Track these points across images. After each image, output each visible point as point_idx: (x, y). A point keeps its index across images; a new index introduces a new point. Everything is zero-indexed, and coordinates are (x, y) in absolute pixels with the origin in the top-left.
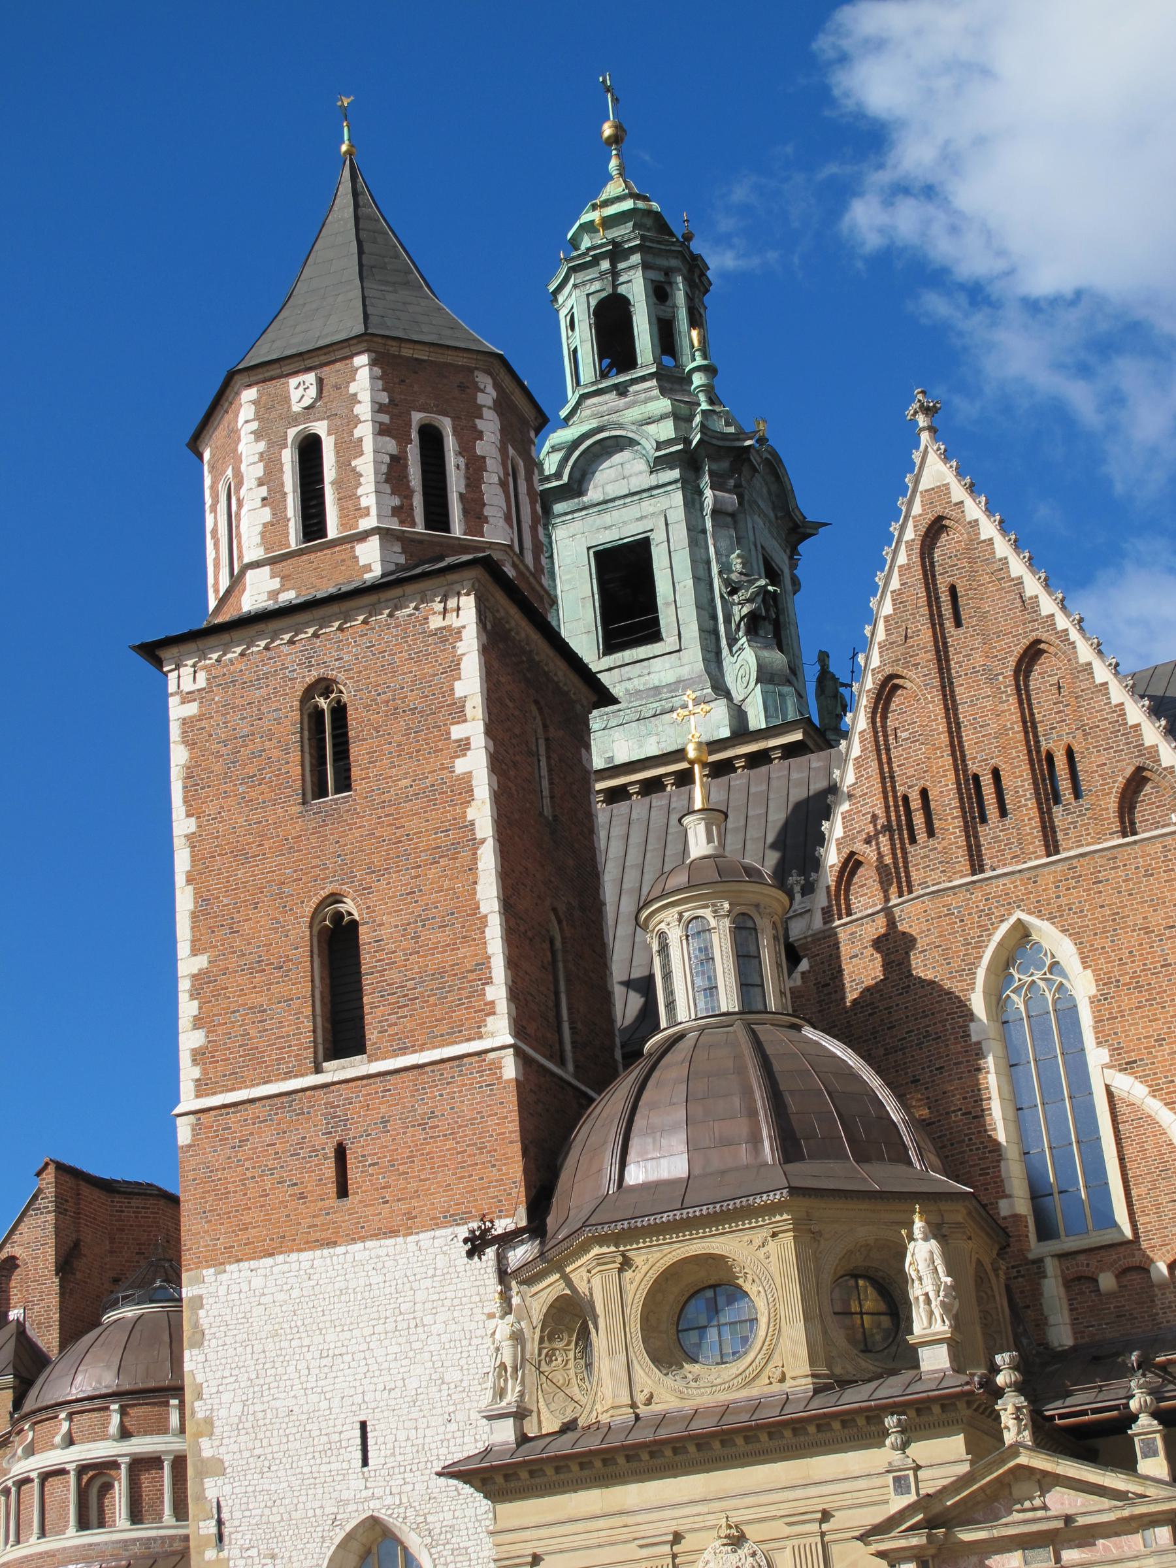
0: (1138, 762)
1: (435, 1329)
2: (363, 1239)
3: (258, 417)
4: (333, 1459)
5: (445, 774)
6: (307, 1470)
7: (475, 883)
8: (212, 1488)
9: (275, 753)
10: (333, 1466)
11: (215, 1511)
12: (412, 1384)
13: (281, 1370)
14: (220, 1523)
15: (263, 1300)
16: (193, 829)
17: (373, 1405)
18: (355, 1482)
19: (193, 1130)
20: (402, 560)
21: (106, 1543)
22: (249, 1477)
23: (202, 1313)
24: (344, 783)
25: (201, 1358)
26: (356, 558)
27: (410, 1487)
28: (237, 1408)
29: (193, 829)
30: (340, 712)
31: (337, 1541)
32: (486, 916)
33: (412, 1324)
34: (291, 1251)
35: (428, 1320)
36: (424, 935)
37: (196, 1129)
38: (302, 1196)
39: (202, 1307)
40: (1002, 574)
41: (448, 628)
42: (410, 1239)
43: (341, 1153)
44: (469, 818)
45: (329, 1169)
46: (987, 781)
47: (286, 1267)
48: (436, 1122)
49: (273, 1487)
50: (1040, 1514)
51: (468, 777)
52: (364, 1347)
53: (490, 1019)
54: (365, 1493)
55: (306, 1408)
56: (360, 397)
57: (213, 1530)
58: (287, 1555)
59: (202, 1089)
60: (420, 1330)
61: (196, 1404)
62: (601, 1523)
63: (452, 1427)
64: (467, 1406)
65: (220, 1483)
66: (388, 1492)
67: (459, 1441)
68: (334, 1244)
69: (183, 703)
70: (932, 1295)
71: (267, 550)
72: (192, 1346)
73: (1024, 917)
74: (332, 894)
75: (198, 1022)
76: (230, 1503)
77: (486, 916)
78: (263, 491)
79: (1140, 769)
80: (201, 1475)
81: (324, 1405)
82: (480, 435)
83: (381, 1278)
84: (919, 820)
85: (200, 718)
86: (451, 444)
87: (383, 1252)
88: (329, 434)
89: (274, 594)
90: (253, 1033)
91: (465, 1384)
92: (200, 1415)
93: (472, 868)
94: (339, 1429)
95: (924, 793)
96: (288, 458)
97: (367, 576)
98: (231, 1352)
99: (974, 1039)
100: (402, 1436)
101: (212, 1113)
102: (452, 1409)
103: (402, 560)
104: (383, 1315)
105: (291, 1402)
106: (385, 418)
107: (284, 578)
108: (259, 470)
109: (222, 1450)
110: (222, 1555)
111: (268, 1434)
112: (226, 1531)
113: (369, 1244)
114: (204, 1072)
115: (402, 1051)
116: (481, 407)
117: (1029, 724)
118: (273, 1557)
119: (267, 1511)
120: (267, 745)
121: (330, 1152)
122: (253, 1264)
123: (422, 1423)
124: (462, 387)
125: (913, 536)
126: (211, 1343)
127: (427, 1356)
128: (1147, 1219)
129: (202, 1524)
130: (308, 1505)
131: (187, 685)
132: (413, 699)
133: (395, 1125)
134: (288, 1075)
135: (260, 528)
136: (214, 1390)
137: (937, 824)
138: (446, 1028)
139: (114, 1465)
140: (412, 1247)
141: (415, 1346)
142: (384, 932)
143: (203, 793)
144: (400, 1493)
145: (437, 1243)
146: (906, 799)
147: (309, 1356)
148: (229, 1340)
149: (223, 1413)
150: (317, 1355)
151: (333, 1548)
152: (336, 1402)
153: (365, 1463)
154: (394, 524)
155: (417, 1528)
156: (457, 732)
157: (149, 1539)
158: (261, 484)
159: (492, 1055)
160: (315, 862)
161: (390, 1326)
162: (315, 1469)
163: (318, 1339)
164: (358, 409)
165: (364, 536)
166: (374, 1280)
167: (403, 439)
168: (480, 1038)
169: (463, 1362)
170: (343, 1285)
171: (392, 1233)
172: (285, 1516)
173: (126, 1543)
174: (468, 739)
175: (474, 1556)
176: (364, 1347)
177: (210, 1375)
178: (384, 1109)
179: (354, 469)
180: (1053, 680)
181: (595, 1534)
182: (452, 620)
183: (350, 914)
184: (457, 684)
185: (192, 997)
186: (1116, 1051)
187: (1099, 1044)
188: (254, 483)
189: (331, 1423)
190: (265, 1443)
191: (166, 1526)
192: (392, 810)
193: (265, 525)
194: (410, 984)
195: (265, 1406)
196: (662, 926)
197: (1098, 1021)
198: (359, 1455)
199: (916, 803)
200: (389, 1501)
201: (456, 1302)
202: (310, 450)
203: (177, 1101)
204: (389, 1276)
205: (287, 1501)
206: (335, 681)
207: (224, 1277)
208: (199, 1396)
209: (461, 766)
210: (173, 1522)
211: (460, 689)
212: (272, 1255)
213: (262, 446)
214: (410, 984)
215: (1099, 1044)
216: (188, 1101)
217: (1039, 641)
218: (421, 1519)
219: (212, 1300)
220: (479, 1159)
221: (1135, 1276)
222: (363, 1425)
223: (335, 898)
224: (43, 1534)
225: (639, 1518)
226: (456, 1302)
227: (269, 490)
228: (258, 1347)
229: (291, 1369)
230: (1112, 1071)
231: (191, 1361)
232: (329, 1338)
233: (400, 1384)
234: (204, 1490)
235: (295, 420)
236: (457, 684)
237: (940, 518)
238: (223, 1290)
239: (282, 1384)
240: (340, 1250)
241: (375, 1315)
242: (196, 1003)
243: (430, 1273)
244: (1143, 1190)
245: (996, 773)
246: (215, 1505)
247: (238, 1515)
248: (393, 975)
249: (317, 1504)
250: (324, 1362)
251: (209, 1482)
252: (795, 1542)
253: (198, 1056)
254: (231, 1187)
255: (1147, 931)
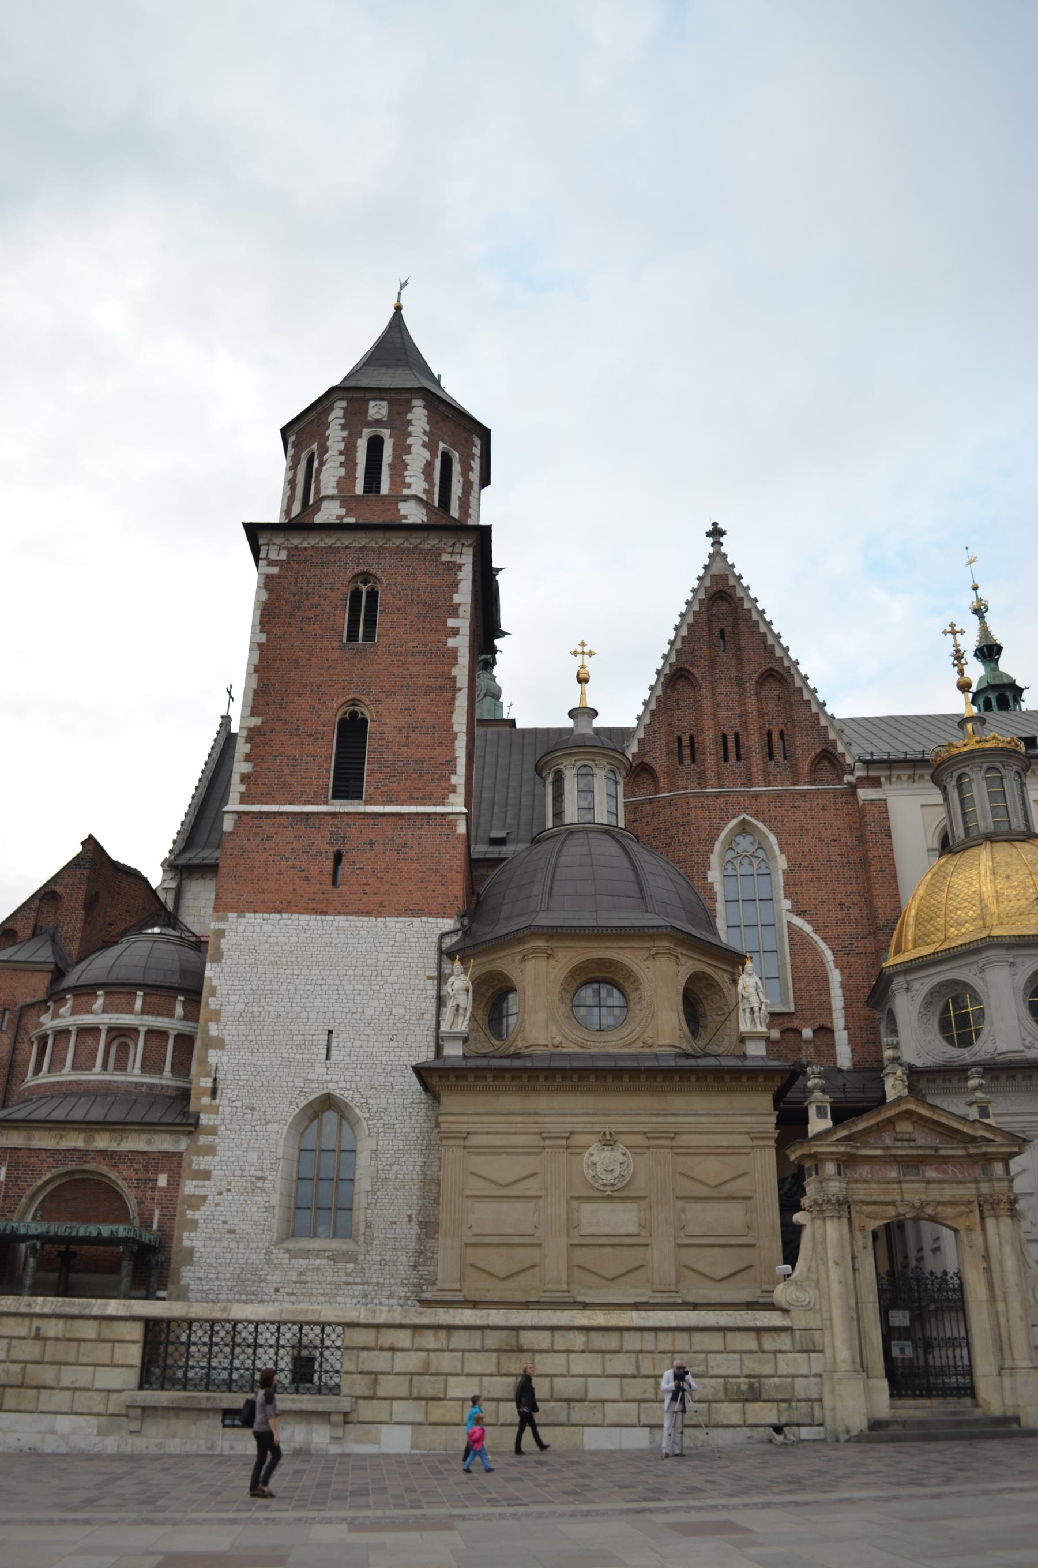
0: (824, 746)
1: (390, 979)
2: (346, 914)
3: (345, 417)
4: (306, 1051)
5: (440, 645)
6: (285, 1055)
7: (452, 712)
8: (213, 1057)
9: (328, 609)
10: (305, 1056)
11: (213, 1072)
12: (370, 1012)
13: (276, 987)
14: (215, 1080)
15: (270, 940)
16: (264, 640)
17: (338, 1021)
18: (320, 1069)
19: (235, 823)
20: (425, 519)
21: (122, 1082)
22: (242, 1053)
23: (223, 941)
24: (370, 636)
25: (218, 970)
26: (398, 510)
27: (358, 1078)
28: (240, 1007)
29: (264, 640)
30: (373, 595)
31: (301, 1106)
32: (456, 734)
33: (374, 973)
34: (294, 912)
35: (386, 972)
36: (413, 736)
37: (237, 824)
38: (307, 879)
39: (224, 937)
40: (754, 629)
41: (454, 562)
42: (379, 919)
43: (338, 858)
44: (453, 673)
45: (328, 865)
46: (731, 738)
47: (289, 922)
48: (407, 850)
49: (259, 1063)
50: (912, 1144)
51: (455, 651)
52: (338, 982)
53: (451, 796)
54: (326, 1078)
55: (290, 1015)
56: (413, 422)
57: (210, 1085)
58: (263, 1109)
59: (244, 799)
60: (379, 978)
61: (210, 999)
62: (519, 1119)
63: (394, 1044)
64: (406, 1032)
65: (220, 1054)
66: (342, 1078)
67: (398, 1054)
68: (326, 913)
69: (268, 565)
70: (756, 1009)
71: (339, 491)
72: (212, 961)
73: (748, 818)
74: (354, 699)
75: (248, 758)
76: (226, 1068)
77: (456, 734)
78: (342, 458)
79: (824, 750)
80: (206, 1047)
81: (304, 1015)
82: (472, 469)
83: (356, 941)
84: (686, 752)
85: (279, 576)
86: (456, 468)
87: (359, 924)
88: (391, 437)
89: (339, 517)
90: (287, 772)
91: (407, 1018)
92: (212, 1007)
93: (451, 703)
94: (312, 1032)
95: (692, 738)
96: (362, 445)
97: (404, 521)
98: (241, 969)
99: (710, 880)
100: (358, 1043)
101: (250, 816)
102: (395, 1032)
103: (425, 519)
104: (354, 964)
105: (280, 1010)
106: (427, 439)
107: (348, 510)
108: (341, 446)
109: (225, 1032)
110: (217, 1101)
111: (261, 1027)
112: (220, 1086)
113: (350, 918)
114: (248, 789)
115: (389, 803)
116: (474, 455)
117: (761, 714)
118: (253, 1109)
119: (252, 1078)
120: (322, 602)
121: (331, 855)
122: (266, 916)
123: (373, 1038)
124: (466, 440)
125: (703, 597)
126: (226, 961)
127: (382, 996)
128: (803, 1002)
129: (202, 1079)
130: (283, 1079)
131: (273, 556)
132: (425, 596)
133: (378, 847)
134: (307, 802)
135: (336, 478)
136: (225, 992)
137: (697, 756)
138: (420, 795)
139: (135, 1031)
140: (381, 925)
141: (374, 988)
142: (384, 728)
143: (274, 621)
144: (351, 1081)
145: (398, 925)
146: (680, 739)
147: (297, 982)
148: (241, 961)
149: (229, 1008)
150: (304, 982)
151: (298, 1110)
152: (313, 1015)
153: (328, 1057)
154: (424, 497)
155: (361, 1108)
156: (451, 622)
157: (153, 1084)
158: (341, 453)
159: (451, 817)
160: (346, 678)
161: (358, 972)
162: (292, 1056)
163: (305, 972)
164: (411, 428)
165: (406, 499)
166: (351, 941)
167: (434, 455)
168: (444, 805)
169: (407, 1004)
170: (328, 940)
171: (368, 914)
172: (265, 1083)
173: (137, 1084)
174: (458, 628)
175: (398, 1130)
176: (338, 982)
177: (223, 982)
178: (372, 836)
179: (404, 461)
180: (776, 693)
181: (514, 1126)
182: (458, 560)
183: (362, 714)
184: (455, 596)
185: (247, 741)
186: (795, 903)
187: (786, 897)
188: (336, 453)
189: (307, 1028)
190: (257, 1032)
191: (167, 1079)
192: (402, 658)
193: (340, 477)
194: (400, 764)
195: (261, 1009)
196: (561, 767)
197: (786, 884)
198: (325, 1051)
199: (686, 742)
200: (342, 1084)
201: (407, 965)
202: (375, 446)
203: (227, 804)
204: (362, 940)
205: (267, 1074)
206: (374, 576)
207: (244, 920)
208: (213, 993)
209: (451, 642)
210: (170, 1075)
211: (457, 599)
212: (279, 912)
213: (345, 433)
214: (400, 764)
215: (786, 897)
216: (234, 805)
217: (771, 669)
218: (363, 1101)
219: (232, 934)
220: (431, 879)
221: (791, 1036)
222: (330, 1032)
223: (354, 702)
224: (74, 1067)
225: (547, 1119)
226: (407, 965)
227: (346, 459)
228: (261, 970)
229: (283, 988)
230: (791, 915)
231: (210, 971)
232: (313, 972)
233: (360, 1010)
234: (207, 1057)
235: (369, 425)
236: (455, 596)
237: (721, 591)
238: (241, 928)
239: (275, 996)
240: (328, 918)
241: (349, 964)
242: (249, 746)
243: (391, 943)
244: (803, 986)
245: (737, 736)
246: (214, 1068)
247: (230, 1077)
248: (389, 756)
249: (289, 1079)
250: (308, 987)
251: (212, 1053)
252: (654, 1150)
253: (245, 778)
254: (257, 864)
255: (821, 840)
